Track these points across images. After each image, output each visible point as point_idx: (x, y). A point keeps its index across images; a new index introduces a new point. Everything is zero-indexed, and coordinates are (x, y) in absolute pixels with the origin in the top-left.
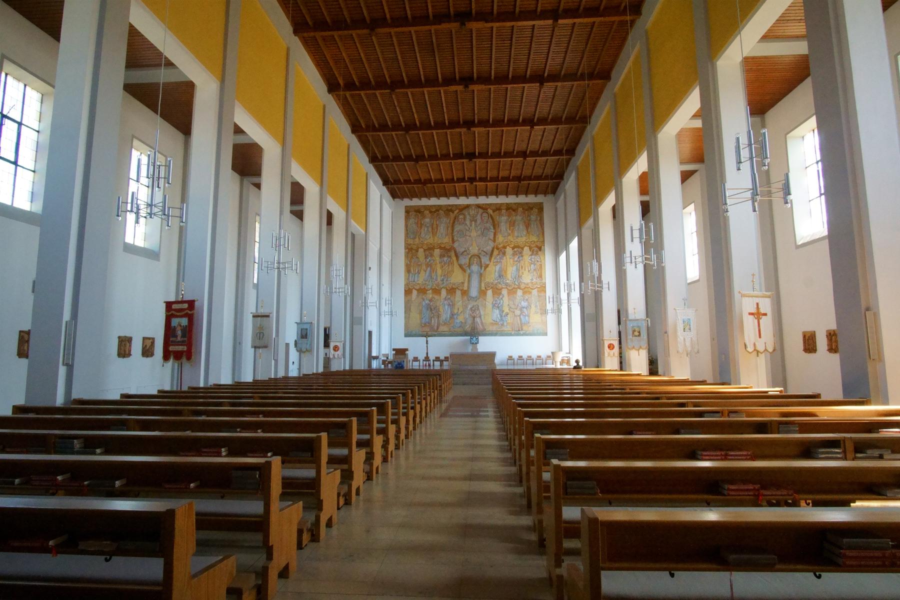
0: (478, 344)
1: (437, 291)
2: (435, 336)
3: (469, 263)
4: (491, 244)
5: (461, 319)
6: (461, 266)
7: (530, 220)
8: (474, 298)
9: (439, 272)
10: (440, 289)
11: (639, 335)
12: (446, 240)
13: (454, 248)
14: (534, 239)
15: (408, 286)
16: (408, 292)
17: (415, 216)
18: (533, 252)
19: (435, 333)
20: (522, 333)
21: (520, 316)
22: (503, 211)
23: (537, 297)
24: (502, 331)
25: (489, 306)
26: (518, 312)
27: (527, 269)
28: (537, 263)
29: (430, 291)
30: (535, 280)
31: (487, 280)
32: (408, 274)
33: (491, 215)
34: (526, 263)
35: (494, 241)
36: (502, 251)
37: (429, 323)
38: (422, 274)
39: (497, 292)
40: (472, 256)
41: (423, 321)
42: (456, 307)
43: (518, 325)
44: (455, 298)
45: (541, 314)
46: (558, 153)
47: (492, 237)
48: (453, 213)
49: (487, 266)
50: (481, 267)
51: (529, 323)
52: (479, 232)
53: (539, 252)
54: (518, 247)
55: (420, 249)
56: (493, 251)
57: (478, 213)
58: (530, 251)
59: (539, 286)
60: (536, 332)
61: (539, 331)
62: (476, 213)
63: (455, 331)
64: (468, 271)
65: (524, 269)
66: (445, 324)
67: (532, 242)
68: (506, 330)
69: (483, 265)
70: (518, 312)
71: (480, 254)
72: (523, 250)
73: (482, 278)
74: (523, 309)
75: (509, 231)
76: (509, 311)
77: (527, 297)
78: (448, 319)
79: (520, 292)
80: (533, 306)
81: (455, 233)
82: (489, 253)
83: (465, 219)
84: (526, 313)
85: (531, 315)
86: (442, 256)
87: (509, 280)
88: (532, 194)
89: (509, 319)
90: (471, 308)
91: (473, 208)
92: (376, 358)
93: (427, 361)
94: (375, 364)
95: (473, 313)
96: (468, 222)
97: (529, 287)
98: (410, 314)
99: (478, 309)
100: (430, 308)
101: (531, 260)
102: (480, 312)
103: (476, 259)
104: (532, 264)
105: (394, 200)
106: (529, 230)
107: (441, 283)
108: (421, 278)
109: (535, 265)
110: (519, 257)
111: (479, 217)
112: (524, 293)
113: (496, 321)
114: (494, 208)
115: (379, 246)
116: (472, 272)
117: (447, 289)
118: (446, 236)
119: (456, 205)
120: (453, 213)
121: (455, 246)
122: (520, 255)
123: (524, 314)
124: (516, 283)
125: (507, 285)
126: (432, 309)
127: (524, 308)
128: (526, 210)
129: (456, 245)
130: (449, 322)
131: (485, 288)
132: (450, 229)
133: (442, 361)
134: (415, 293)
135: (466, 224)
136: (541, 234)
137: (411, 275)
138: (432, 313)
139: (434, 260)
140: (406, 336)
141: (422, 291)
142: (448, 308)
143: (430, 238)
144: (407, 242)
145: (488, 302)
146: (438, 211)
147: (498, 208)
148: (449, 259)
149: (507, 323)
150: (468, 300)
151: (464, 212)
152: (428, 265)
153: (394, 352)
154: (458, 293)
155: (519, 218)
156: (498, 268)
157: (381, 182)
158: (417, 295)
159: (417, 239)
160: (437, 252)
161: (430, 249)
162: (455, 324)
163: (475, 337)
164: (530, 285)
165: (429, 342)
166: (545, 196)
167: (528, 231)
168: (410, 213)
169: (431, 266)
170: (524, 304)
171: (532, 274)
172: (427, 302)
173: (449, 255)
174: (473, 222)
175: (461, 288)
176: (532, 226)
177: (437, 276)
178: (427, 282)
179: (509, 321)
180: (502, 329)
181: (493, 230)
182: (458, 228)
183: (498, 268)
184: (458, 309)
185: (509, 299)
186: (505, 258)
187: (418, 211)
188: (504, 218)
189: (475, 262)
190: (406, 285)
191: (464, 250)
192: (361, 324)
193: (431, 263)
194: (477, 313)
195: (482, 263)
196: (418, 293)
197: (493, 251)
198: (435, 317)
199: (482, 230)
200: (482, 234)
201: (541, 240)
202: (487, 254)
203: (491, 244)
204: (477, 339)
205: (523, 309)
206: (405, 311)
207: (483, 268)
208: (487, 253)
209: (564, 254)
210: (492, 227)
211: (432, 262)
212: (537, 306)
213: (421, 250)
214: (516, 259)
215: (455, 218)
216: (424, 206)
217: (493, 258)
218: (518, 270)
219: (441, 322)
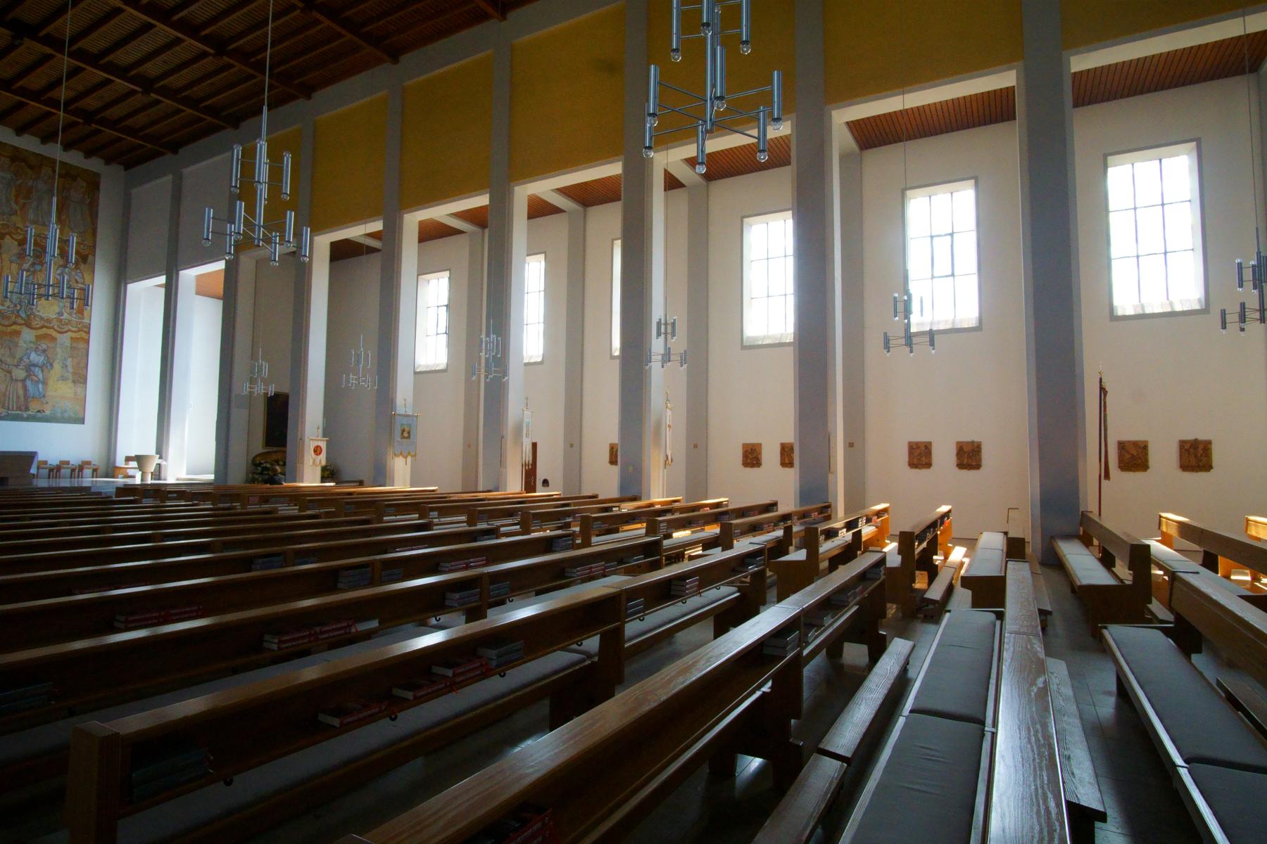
11: (409, 437)
20: (25, 415)
21: (24, 381)
23: (69, 350)
26: (20, 373)
30: (66, 316)
43: (18, 397)
51: (44, 396)
53: (82, 266)
59: (74, 329)
60: (59, 415)
61: (66, 415)
70: (20, 373)
74: (32, 368)
77: (44, 346)
80: (57, 366)
84: (40, 376)
85: (51, 382)
97: (53, 328)
110: (33, 264)
123: (35, 378)
124: (24, 315)
127: (35, 366)
164: (55, 324)
170: (34, 357)
205: (32, 368)
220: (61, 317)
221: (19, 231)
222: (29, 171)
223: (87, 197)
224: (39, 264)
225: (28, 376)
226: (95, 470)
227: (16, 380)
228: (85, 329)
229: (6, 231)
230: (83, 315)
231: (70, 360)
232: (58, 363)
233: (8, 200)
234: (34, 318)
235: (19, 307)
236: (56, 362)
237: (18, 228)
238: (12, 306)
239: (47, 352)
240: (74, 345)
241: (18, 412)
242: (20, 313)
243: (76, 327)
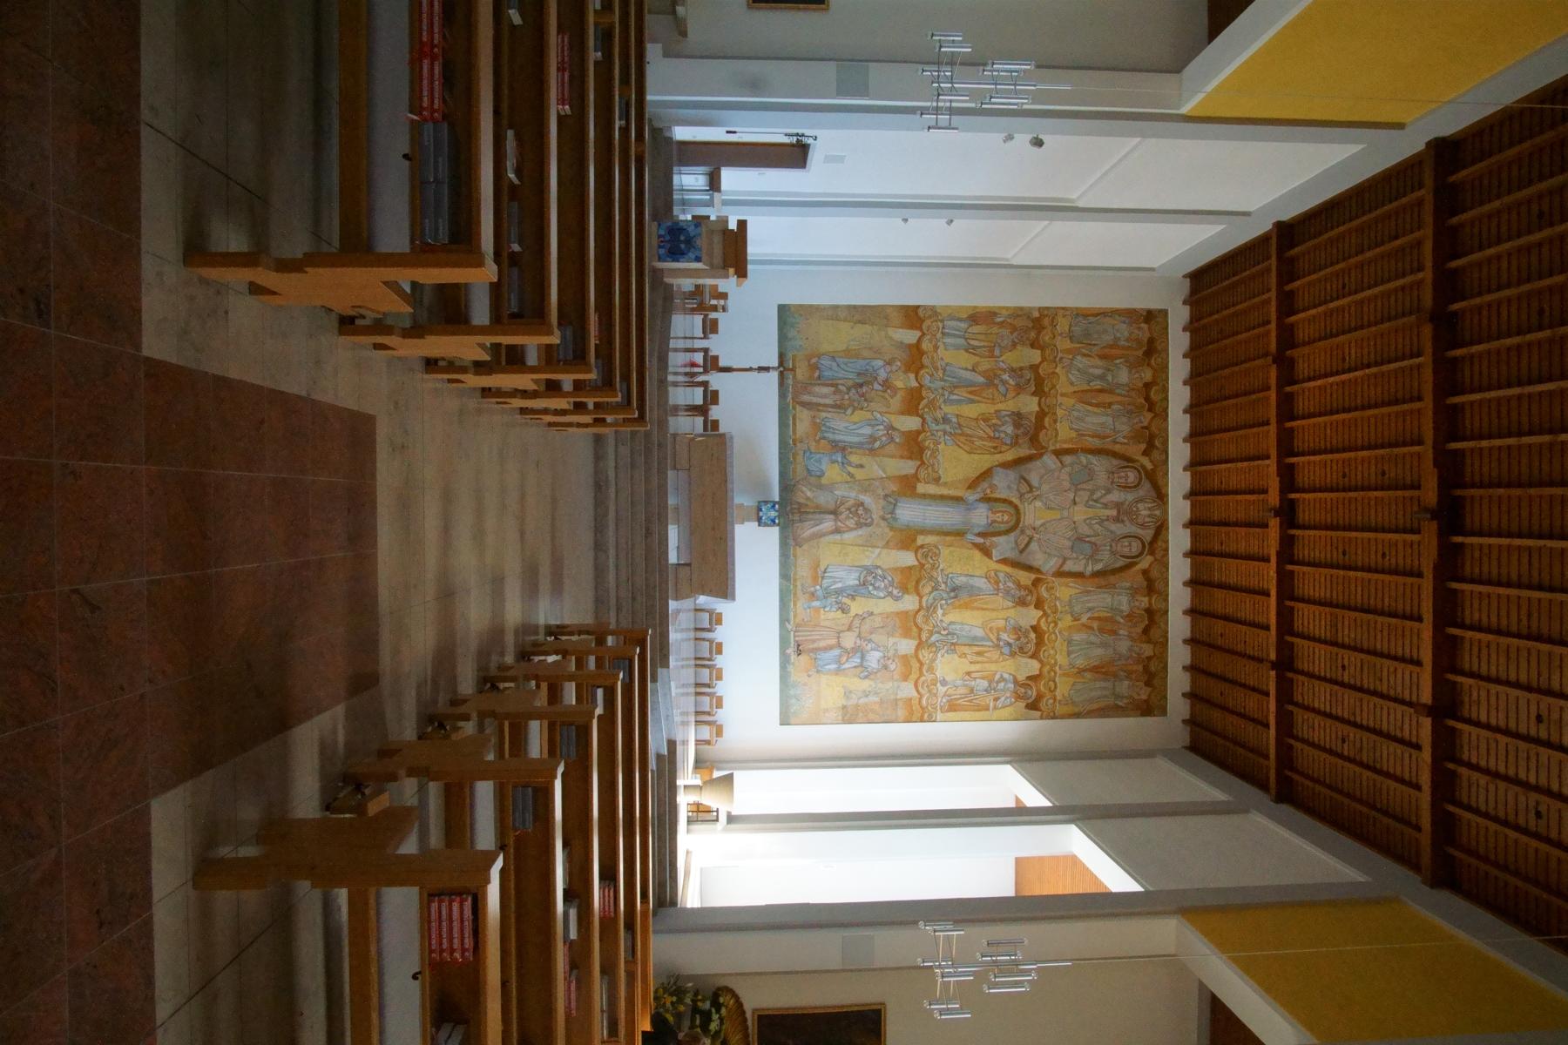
0: (757, 523)
1: (913, 401)
2: (782, 395)
3: (996, 500)
4: (1050, 565)
5: (832, 473)
6: (986, 474)
7: (1115, 676)
8: (892, 512)
9: (971, 411)
10: (920, 412)
12: (1064, 432)
13: (1041, 455)
14: (1063, 688)
15: (930, 317)
16: (913, 316)
17: (1138, 341)
18: (1022, 685)
19: (790, 396)
20: (788, 651)
21: (839, 645)
22: (1146, 599)
23: (892, 697)
24: (795, 594)
25: (870, 557)
26: (849, 640)
27: (973, 668)
28: (992, 698)
29: (914, 384)
30: (942, 690)
31: (945, 552)
32: (965, 316)
33: (1135, 564)
34: (993, 667)
35: (1060, 574)
36: (1031, 595)
37: (819, 378)
38: (965, 360)
39: (910, 581)
40: (1016, 507)
41: (826, 362)
42: (865, 460)
43: (814, 641)
44: (892, 457)
45: (844, 707)
46: (1445, 827)
47: (1070, 566)
48: (1146, 453)
49: (986, 552)
50: (980, 535)
51: (818, 672)
52: (1084, 530)
53: (1022, 704)
54: (1040, 642)
55: (1039, 352)
56: (1029, 568)
57: (1143, 526)
58: (1029, 678)
59: (924, 702)
60: (792, 692)
62: (1140, 520)
63: (794, 455)
64: (971, 497)
65: (976, 658)
66: (817, 426)
67: (1051, 683)
68: (799, 604)
69: (988, 542)
70: (849, 640)
71: (1023, 532)
72: (1033, 656)
73: (948, 538)
74: (859, 655)
75: (1089, 615)
76: (852, 613)
77: (893, 667)
78: (830, 436)
79: (906, 646)
80: (866, 685)
81: (1083, 459)
82: (1023, 559)
83: (1126, 487)
84: (846, 666)
86: (1018, 418)
87: (943, 615)
88: (1193, 682)
89: (831, 616)
90: (862, 504)
91: (1157, 513)
92: (714, 184)
93: (705, 366)
94: (690, 180)
95: (849, 509)
96: (1116, 496)
98: (845, 320)
99: (859, 525)
100: (864, 382)
101: (1002, 679)
102: (851, 529)
103: (1006, 518)
104: (990, 682)
105: (1185, 276)
106: (1088, 675)
107: (939, 415)
108: (952, 357)
109: (986, 690)
110: (1010, 645)
111: (1130, 528)
112: (905, 659)
113: (823, 578)
114: (1154, 574)
115: (1081, 204)
116: (969, 507)
117: (918, 433)
118: (1076, 430)
119: (1166, 461)
120: (1146, 453)
121: (1045, 458)
122: (1015, 648)
124: (933, 639)
125: (931, 609)
126: (862, 388)
127: (863, 658)
128: (1146, 669)
129: (1049, 460)
130: (824, 438)
131: (922, 547)
132: (1096, 443)
133: (702, 410)
134: (910, 336)
135: (1109, 491)
136: (1076, 710)
137: (963, 325)
138: (849, 389)
139: (1005, 396)
140: (783, 310)
141: (915, 358)
142: (859, 435)
143: (1072, 384)
144: (1061, 313)
145: (879, 554)
146: (1150, 410)
147: (1154, 585)
148: (1009, 442)
149: (817, 610)
150: (886, 496)
151: (1146, 485)
152: (991, 379)
153: (733, 225)
154: (908, 467)
155: (1124, 646)
156: (981, 583)
157: (1286, 216)
158: (901, 343)
159: (1067, 344)
160: (1030, 405)
161: (1039, 384)
162: (818, 456)
163: (779, 516)
164: (928, 677)
165: (764, 375)
166: (1184, 721)
167: (1084, 670)
168: (1145, 326)
169: (990, 383)
170: (874, 658)
171: (959, 682)
172: (882, 375)
173: (1020, 441)
174: (1114, 513)
175: (922, 474)
176: (1098, 684)
177: (959, 402)
178: (940, 373)
179: (822, 617)
180: (799, 592)
181: (1090, 568)
182: (1100, 465)
183: (981, 583)
184: (862, 466)
185: (888, 616)
186: (1010, 604)
187: (1153, 350)
188: (1124, 602)
189: (998, 517)
190: (933, 312)
191: (1035, 483)
192: (841, 93)
193: (996, 386)
194: (847, 523)
195: (994, 539)
196: (910, 346)
197: (1029, 568)
198: (837, 397)
199: (1093, 539)
200: (1080, 539)
201: (1059, 709)
202: (1021, 552)
203: (1050, 565)
204: (773, 521)
205: (859, 655)
206: (855, 307)
207: (981, 540)
208: (1024, 554)
209: (1035, 798)
210: (1099, 567)
211: (1002, 389)
212: (867, 696)
213: (1035, 356)
214: (1004, 636)
215: (1128, 459)
216: (1164, 368)
217: (1009, 569)
218: (973, 642)
219: (824, 415)
220: (939, 685)
221: (1052, 625)
222: (1139, 630)
223: (1125, 701)
225: (846, 651)
226: (708, 742)
227: (839, 637)
228: (926, 716)
229: (1049, 612)
230: (948, 711)
231: (876, 699)
232: (870, 686)
233: (1090, 609)
235: (943, 632)
236: (872, 683)
237: (1056, 624)
238: (945, 625)
239: (884, 671)
240: (900, 704)
241: (793, 643)
242: (937, 635)
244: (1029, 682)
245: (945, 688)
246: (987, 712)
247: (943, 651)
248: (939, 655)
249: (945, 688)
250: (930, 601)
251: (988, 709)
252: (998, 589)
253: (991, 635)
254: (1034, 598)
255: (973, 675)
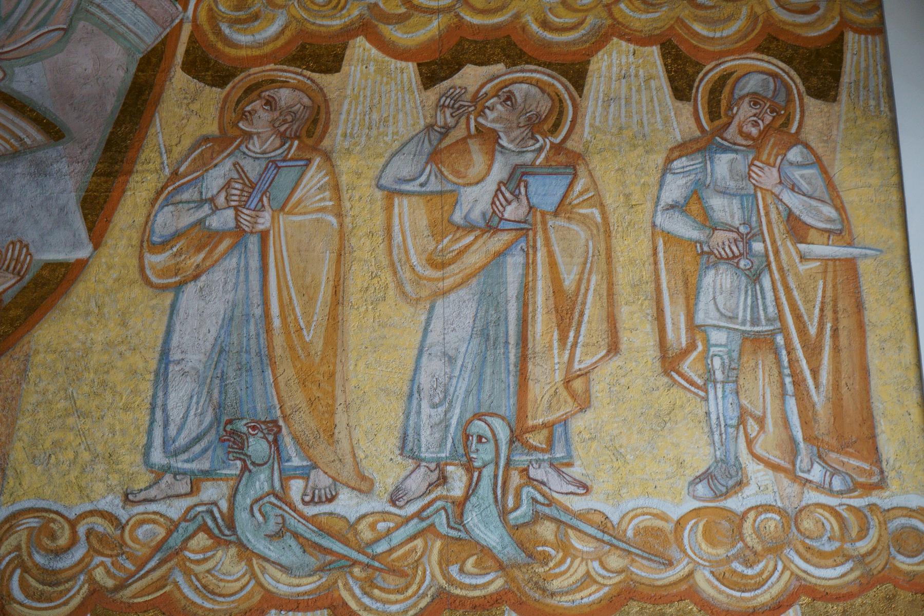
28: (789, 250)
58: (681, 92)
109: (755, 278)
186: (315, 177)
220: (735, 504)
224: (550, 170)
230: (874, 454)
234: (564, 547)
235: (457, 488)
238: (417, 482)
242: (472, 518)
243: (841, 556)
244: (701, 92)
245: (754, 469)
246: (865, 267)
247: (555, 483)
248: (578, 504)
249: (754, 469)
250: (289, 552)
251: (850, 266)
252: (239, 233)
253: (474, 259)
254: (292, 74)
255: (678, 335)
